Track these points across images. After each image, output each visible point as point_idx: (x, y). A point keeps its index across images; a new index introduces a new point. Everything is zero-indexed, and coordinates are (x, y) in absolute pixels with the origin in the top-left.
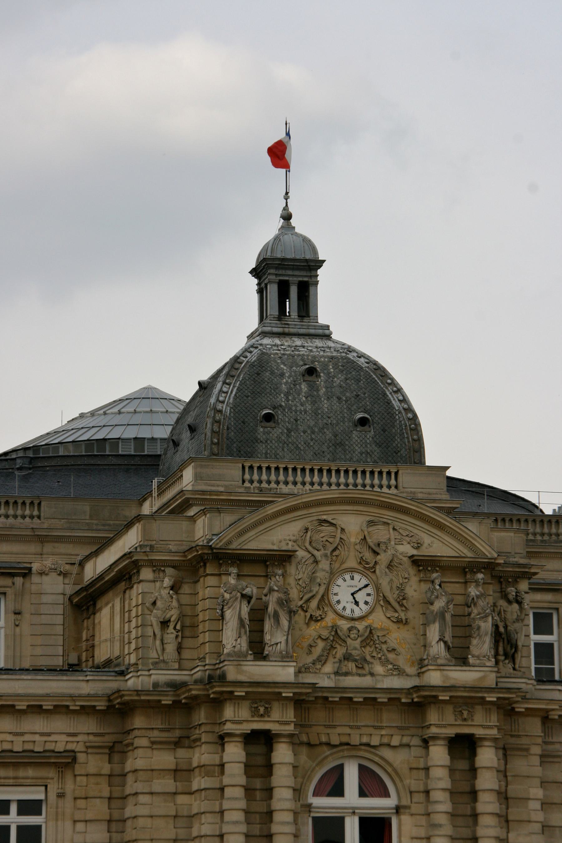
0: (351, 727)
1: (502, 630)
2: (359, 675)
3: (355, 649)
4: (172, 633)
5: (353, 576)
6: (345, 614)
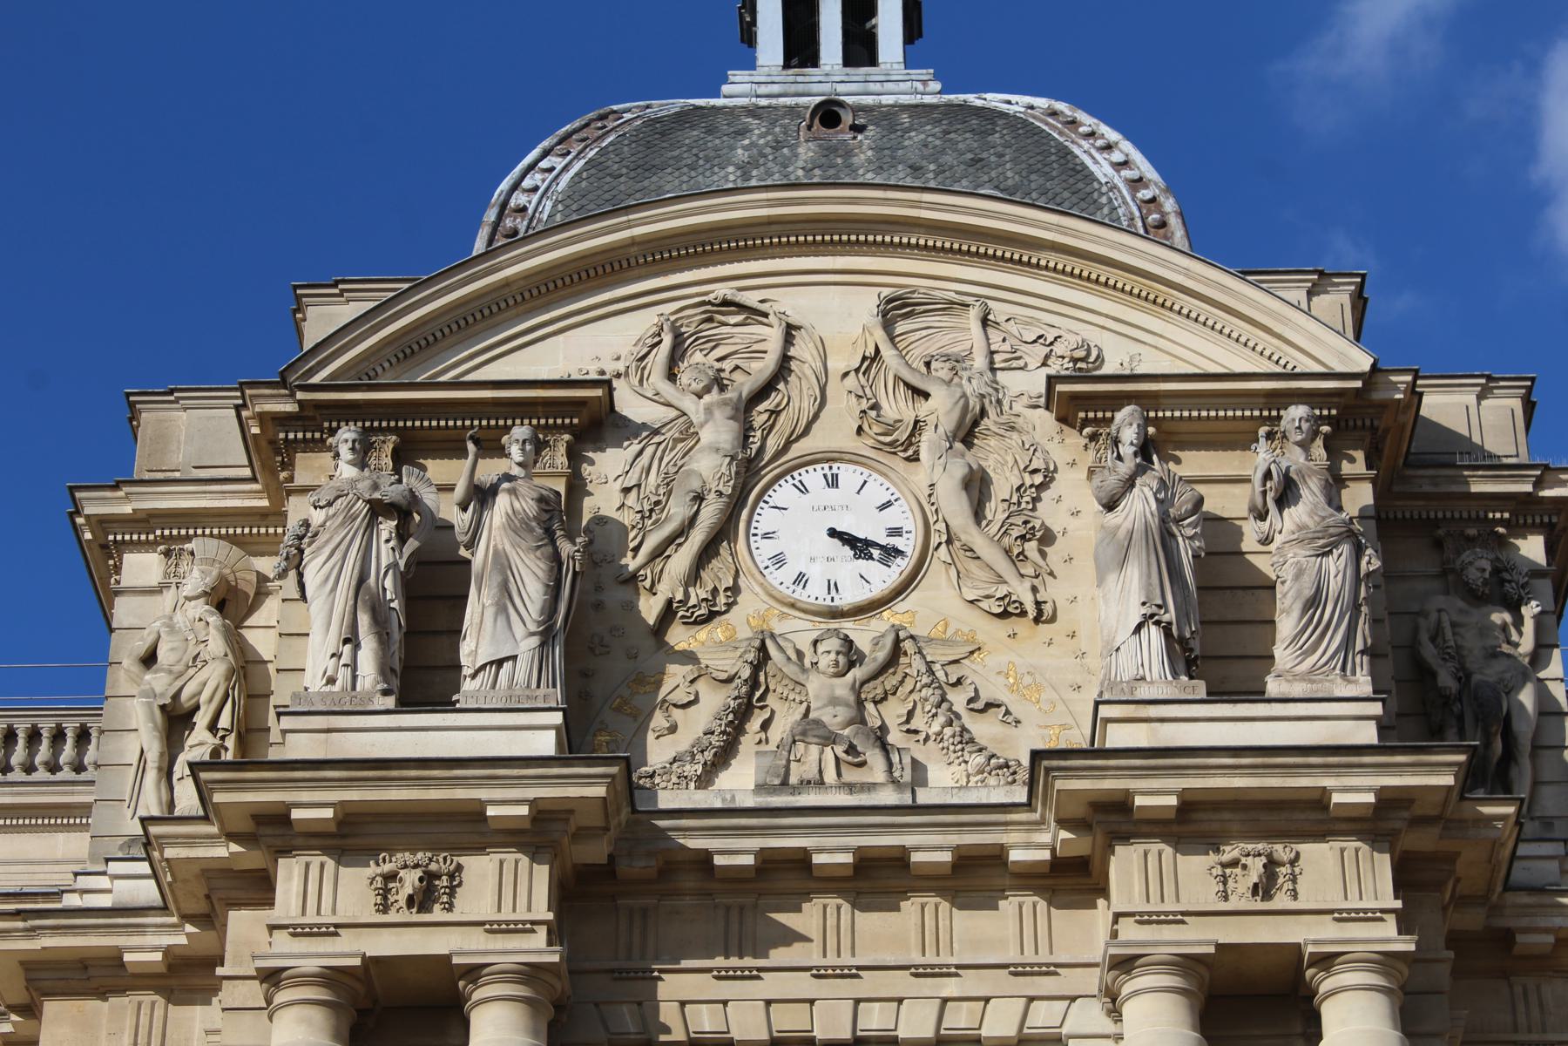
0: (820, 974)
1: (1446, 680)
2: (851, 788)
3: (834, 701)
4: (201, 744)
5: (835, 477)
6: (804, 598)
